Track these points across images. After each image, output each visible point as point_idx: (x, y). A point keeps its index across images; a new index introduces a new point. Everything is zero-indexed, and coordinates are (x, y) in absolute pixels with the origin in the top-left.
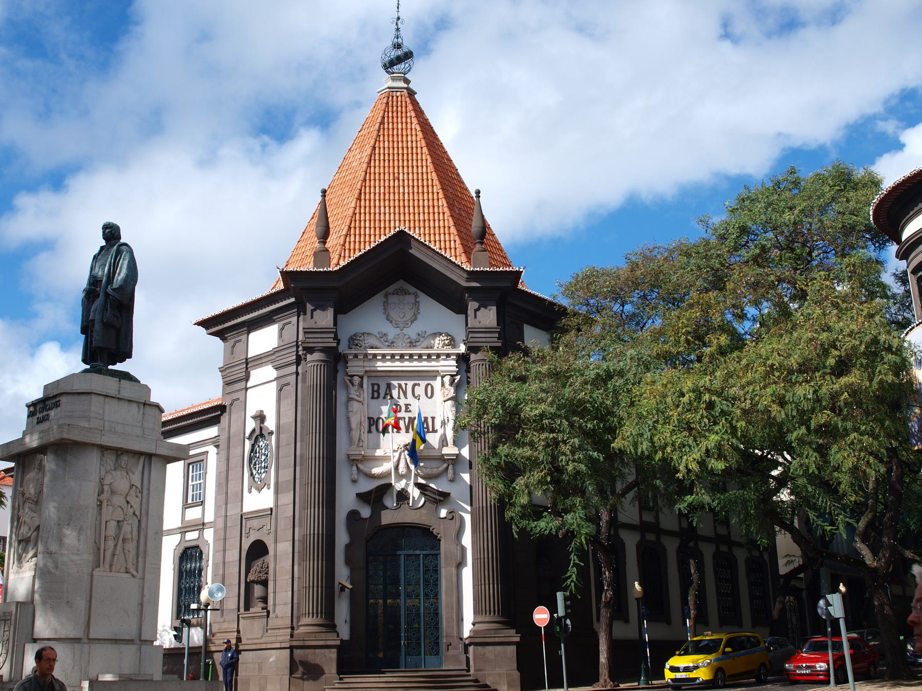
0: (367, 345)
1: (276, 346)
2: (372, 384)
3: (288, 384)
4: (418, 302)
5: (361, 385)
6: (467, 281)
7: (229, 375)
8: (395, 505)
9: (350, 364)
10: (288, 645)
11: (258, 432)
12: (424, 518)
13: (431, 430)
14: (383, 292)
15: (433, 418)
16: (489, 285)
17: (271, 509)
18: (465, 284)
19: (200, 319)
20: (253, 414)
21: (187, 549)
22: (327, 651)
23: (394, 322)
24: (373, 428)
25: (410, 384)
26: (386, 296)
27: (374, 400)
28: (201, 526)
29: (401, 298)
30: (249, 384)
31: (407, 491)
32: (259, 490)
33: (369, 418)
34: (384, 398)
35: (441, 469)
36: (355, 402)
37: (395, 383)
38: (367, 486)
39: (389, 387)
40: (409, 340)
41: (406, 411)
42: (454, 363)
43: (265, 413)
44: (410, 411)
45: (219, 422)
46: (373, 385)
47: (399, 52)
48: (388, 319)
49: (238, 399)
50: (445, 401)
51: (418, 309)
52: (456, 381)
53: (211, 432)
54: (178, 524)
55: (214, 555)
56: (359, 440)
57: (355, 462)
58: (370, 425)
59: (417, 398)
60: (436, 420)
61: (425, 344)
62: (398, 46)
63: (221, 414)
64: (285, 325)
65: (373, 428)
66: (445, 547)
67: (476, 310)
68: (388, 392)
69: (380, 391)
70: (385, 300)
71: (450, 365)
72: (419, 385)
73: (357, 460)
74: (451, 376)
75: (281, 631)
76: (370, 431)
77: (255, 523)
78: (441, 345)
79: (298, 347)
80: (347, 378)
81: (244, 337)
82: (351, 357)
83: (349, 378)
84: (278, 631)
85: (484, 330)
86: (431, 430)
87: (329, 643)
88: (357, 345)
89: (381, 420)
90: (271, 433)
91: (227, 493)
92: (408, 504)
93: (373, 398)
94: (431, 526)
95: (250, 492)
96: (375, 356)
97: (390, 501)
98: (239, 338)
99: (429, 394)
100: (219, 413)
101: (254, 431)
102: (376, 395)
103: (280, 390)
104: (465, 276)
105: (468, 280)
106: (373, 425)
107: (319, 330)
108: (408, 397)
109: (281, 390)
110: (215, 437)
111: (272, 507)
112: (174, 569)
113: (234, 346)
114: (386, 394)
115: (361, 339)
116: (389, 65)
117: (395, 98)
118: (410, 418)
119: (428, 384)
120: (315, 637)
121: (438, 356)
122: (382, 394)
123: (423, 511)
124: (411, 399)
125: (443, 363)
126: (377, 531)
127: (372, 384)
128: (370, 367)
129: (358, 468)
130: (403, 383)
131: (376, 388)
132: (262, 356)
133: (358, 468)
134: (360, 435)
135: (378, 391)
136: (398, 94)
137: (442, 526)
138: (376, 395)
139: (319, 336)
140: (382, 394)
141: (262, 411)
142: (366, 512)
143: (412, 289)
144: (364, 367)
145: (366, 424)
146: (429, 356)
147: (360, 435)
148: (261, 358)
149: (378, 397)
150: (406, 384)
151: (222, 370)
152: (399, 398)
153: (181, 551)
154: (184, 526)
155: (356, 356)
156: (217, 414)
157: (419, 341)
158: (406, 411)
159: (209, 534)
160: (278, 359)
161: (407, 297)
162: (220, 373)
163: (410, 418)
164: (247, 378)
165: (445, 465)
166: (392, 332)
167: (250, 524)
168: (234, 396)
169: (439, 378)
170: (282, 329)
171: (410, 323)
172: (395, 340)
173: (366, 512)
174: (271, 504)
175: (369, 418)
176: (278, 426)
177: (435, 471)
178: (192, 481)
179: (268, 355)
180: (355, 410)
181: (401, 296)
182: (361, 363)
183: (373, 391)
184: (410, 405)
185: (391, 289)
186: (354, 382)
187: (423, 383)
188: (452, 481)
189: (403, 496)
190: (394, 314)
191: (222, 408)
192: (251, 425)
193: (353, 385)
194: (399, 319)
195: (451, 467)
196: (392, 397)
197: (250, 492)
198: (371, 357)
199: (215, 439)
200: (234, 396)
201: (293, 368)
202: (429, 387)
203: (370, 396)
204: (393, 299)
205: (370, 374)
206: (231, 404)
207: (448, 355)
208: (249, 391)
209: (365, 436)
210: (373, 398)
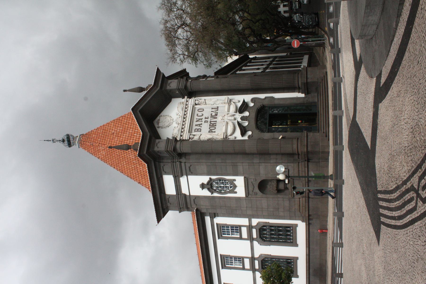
0: (178, 133)
1: (172, 176)
2: (195, 132)
3: (189, 168)
4: (164, 116)
5: (194, 135)
6: (158, 88)
7: (183, 207)
8: (247, 121)
9: (184, 139)
10: (306, 162)
11: (209, 187)
12: (253, 111)
13: (217, 109)
14: (157, 129)
15: (212, 109)
16: (161, 80)
17: (245, 177)
18: (159, 88)
19: (157, 221)
20: (201, 189)
21: (260, 237)
22: (309, 137)
23: (170, 124)
24: (213, 131)
25: (196, 117)
26: (159, 127)
27: (201, 131)
28: (250, 228)
29: (161, 121)
30: (188, 194)
31: (242, 117)
32: (235, 187)
33: (209, 132)
34: (201, 127)
35: (234, 104)
36: (201, 137)
37: (195, 123)
38: (238, 131)
39: (196, 125)
40: (179, 118)
41: (208, 119)
42: (190, 100)
43: (201, 183)
44: (208, 117)
45: (203, 213)
46: (195, 131)
47: (66, 139)
48: (169, 127)
49: (194, 200)
50: (206, 103)
51: (167, 115)
52: (198, 99)
53: (208, 219)
54: (248, 242)
55: (264, 218)
56: (218, 136)
57: (227, 136)
58: (212, 132)
59: (203, 115)
60: (213, 108)
61: (181, 112)
62: (63, 141)
63: (200, 212)
64: (163, 170)
65: (213, 131)
66: (266, 103)
67: (170, 87)
68: (199, 125)
69: (198, 128)
70: (160, 128)
71: (191, 101)
72: (197, 114)
73: (226, 136)
74: (196, 100)
75: (300, 169)
76: (215, 132)
77: (251, 189)
78: (183, 105)
79: (173, 162)
80: (190, 140)
81: (167, 197)
82: (181, 138)
83: (190, 139)
84: (300, 171)
85: (179, 83)
86: (217, 109)
87: (306, 135)
88: (177, 137)
89: (211, 128)
90: (210, 179)
91: (236, 207)
92: (246, 116)
93: (200, 131)
94: (257, 108)
95: (236, 193)
96: (182, 128)
97: (246, 124)
98: (167, 199)
99: (202, 110)
100: (199, 213)
101: (209, 189)
102: (199, 130)
103: (192, 174)
104: (156, 87)
105: (157, 87)
106: (212, 131)
107: (167, 144)
108: (201, 118)
109: (192, 173)
110: (210, 217)
111: (243, 177)
112: (270, 245)
113: (171, 204)
114: (200, 126)
115: (174, 134)
116: (70, 145)
117: (82, 139)
118: (211, 117)
119: (198, 110)
120: (303, 142)
121: (186, 105)
122: (199, 128)
123: (251, 111)
124: (203, 117)
125: (190, 103)
126: (257, 128)
127: (195, 132)
128: (187, 131)
129: (230, 135)
130: (195, 120)
131: (196, 130)
132: (176, 185)
133: (230, 135)
134: (216, 135)
135: (198, 129)
136: (81, 139)
137: (258, 104)
138: (199, 130)
139: (169, 145)
140: (199, 128)
141: (200, 185)
142: (250, 133)
143: (158, 118)
144: (186, 133)
145: (211, 133)
146: (186, 108)
147: (216, 135)
148: (177, 186)
149: (201, 129)
150: (197, 119)
151: (180, 212)
152: (202, 121)
153: (261, 240)
154: (250, 239)
155: (181, 136)
156: (200, 214)
157: (180, 115)
158: (208, 119)
159: (255, 222)
160: (178, 175)
161: (160, 120)
162: (182, 212)
163: (211, 117)
164: (185, 195)
165: (232, 103)
166: (175, 125)
167: (251, 192)
168: (192, 203)
169: (196, 106)
170: (165, 172)
171: (171, 118)
172: (177, 123)
173: (250, 133)
174: (242, 178)
175: (209, 132)
176: (208, 174)
177: (235, 106)
178: (229, 234)
179: (176, 181)
180: (205, 136)
181: (160, 121)
182: (185, 134)
183: (198, 131)
184: (205, 117)
185: (156, 126)
186: (192, 137)
187: (197, 112)
188: (239, 101)
189: (243, 118)
190: (167, 124)
191: (197, 210)
192: (206, 193)
193: (193, 138)
194: (169, 122)
195: (233, 101)
196: (201, 124)
197: (236, 193)
198: (183, 130)
199: (211, 218)
200: (192, 203)
201: (183, 164)
202: (199, 110)
203: (200, 132)
204: (160, 125)
205: (190, 132)
206: (196, 205)
207: (187, 101)
208: (191, 194)
209: (216, 133)
210: (200, 131)
